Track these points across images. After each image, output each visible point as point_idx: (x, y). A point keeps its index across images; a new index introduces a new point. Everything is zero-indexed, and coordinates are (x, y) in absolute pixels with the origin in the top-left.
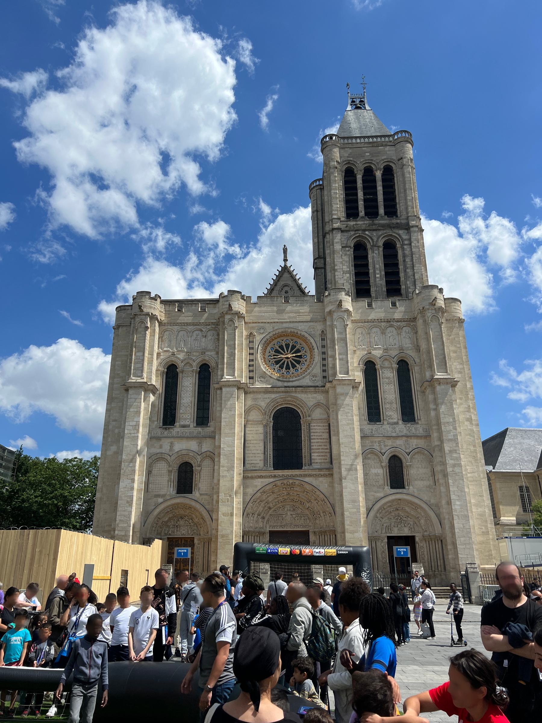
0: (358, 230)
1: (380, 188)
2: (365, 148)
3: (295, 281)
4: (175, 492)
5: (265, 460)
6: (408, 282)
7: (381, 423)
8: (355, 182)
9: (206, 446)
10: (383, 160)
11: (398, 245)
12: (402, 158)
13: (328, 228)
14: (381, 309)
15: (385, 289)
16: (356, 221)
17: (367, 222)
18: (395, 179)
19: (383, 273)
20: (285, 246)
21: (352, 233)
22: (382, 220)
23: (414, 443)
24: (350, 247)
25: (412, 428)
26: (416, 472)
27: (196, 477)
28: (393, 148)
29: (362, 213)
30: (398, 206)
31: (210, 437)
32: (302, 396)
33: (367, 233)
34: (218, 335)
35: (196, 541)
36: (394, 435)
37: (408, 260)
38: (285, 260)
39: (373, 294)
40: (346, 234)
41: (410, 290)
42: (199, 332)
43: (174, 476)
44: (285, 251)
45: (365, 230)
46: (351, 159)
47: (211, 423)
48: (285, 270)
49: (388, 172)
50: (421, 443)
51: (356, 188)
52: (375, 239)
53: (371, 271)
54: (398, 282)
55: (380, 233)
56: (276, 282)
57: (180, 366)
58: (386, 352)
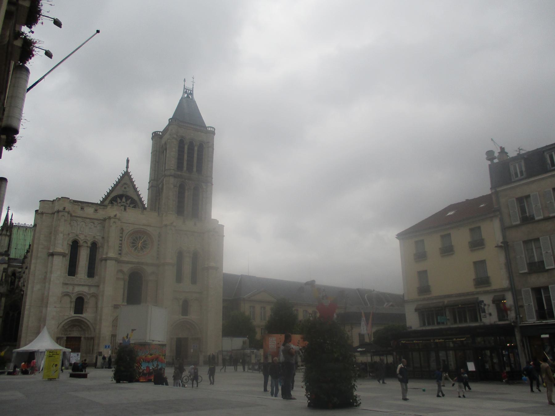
1: (196, 156)
3: (132, 182)
5: (123, 299)
8: (184, 148)
9: (93, 290)
27: (85, 306)
29: (185, 169)
31: (96, 286)
34: (104, 227)
35: (82, 339)
38: (127, 167)
42: (92, 224)
43: (73, 305)
44: (128, 161)
47: (96, 278)
51: (184, 152)
57: (81, 242)
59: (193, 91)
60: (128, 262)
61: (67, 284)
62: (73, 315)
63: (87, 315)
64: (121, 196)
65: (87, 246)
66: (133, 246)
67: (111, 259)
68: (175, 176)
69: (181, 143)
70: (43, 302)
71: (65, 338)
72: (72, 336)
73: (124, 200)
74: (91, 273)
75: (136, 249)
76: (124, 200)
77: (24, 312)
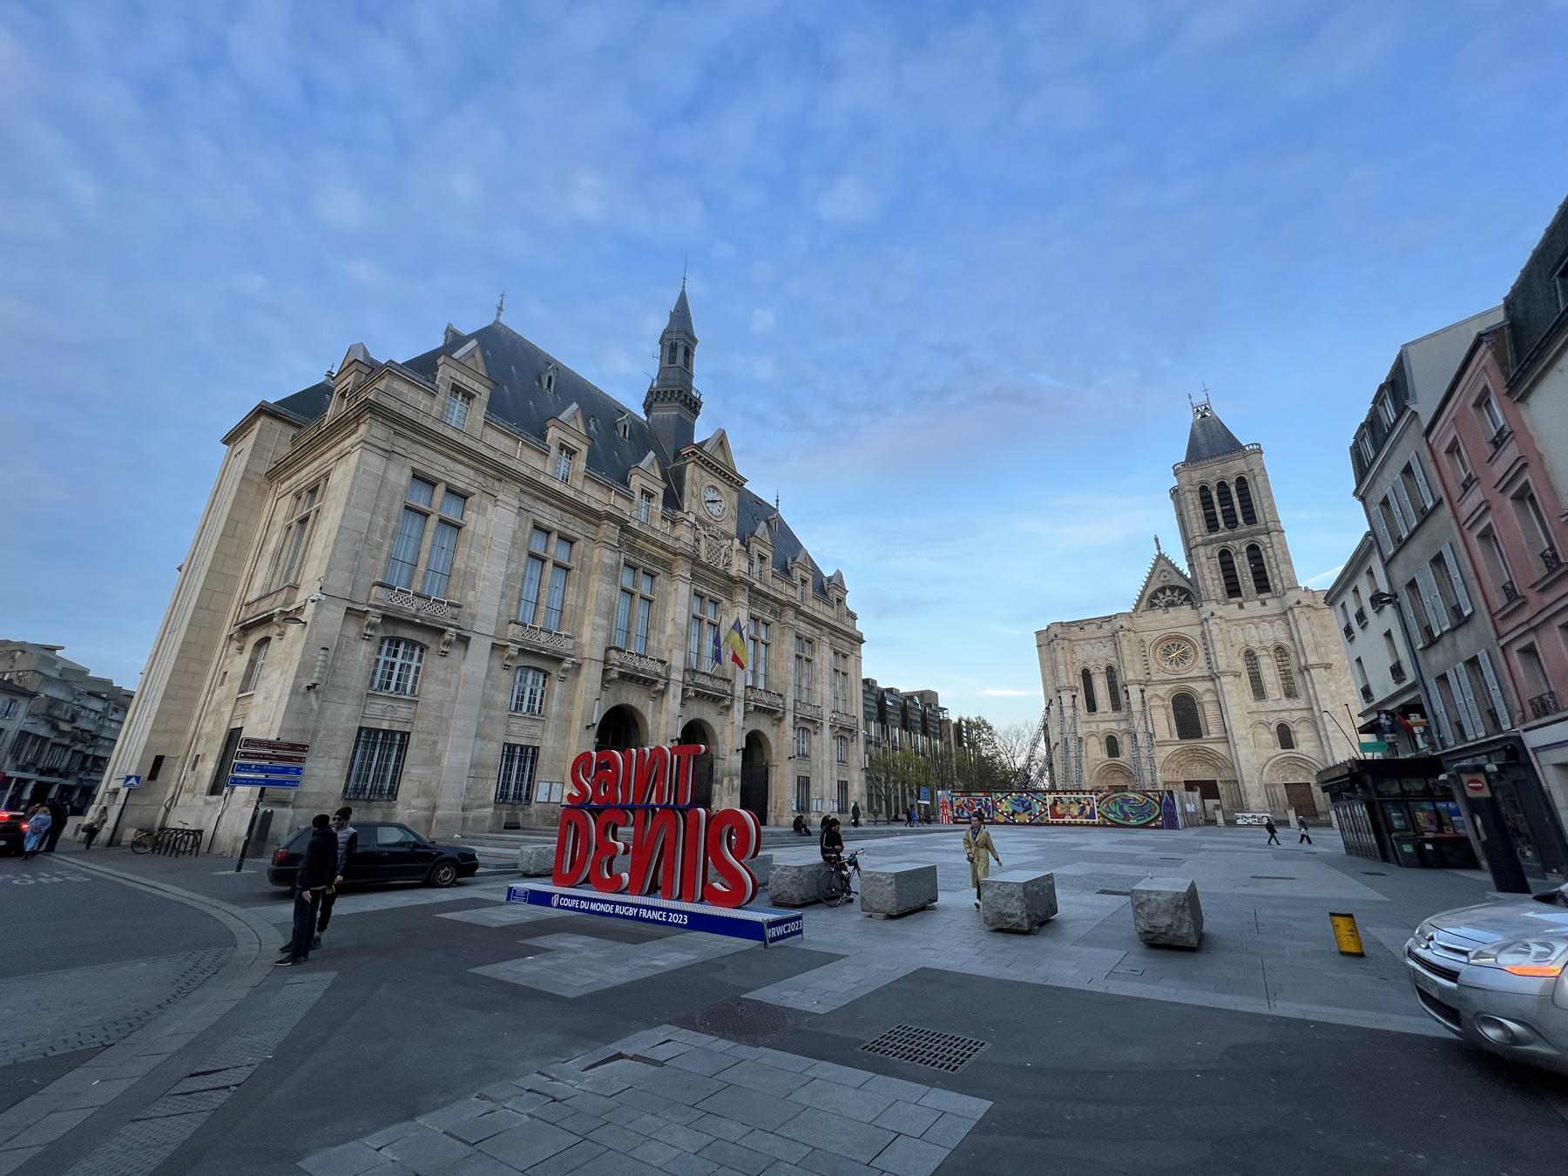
1: (1236, 500)
3: (1173, 566)
9: (1123, 726)
13: (1192, 544)
14: (1253, 607)
17: (1228, 533)
22: (1243, 528)
23: (1297, 715)
25: (1295, 703)
26: (1302, 735)
29: (1222, 525)
32: (1192, 685)
40: (1209, 548)
43: (1104, 746)
44: (1157, 540)
48: (1161, 557)
49: (1241, 482)
50: (1305, 714)
54: (1266, 579)
56: (1153, 570)
57: (1092, 670)
60: (1164, 682)
62: (1105, 756)
63: (1124, 757)
64: (1162, 590)
68: (1205, 544)
69: (1204, 491)
73: (1168, 592)
74: (1116, 706)
76: (1168, 592)
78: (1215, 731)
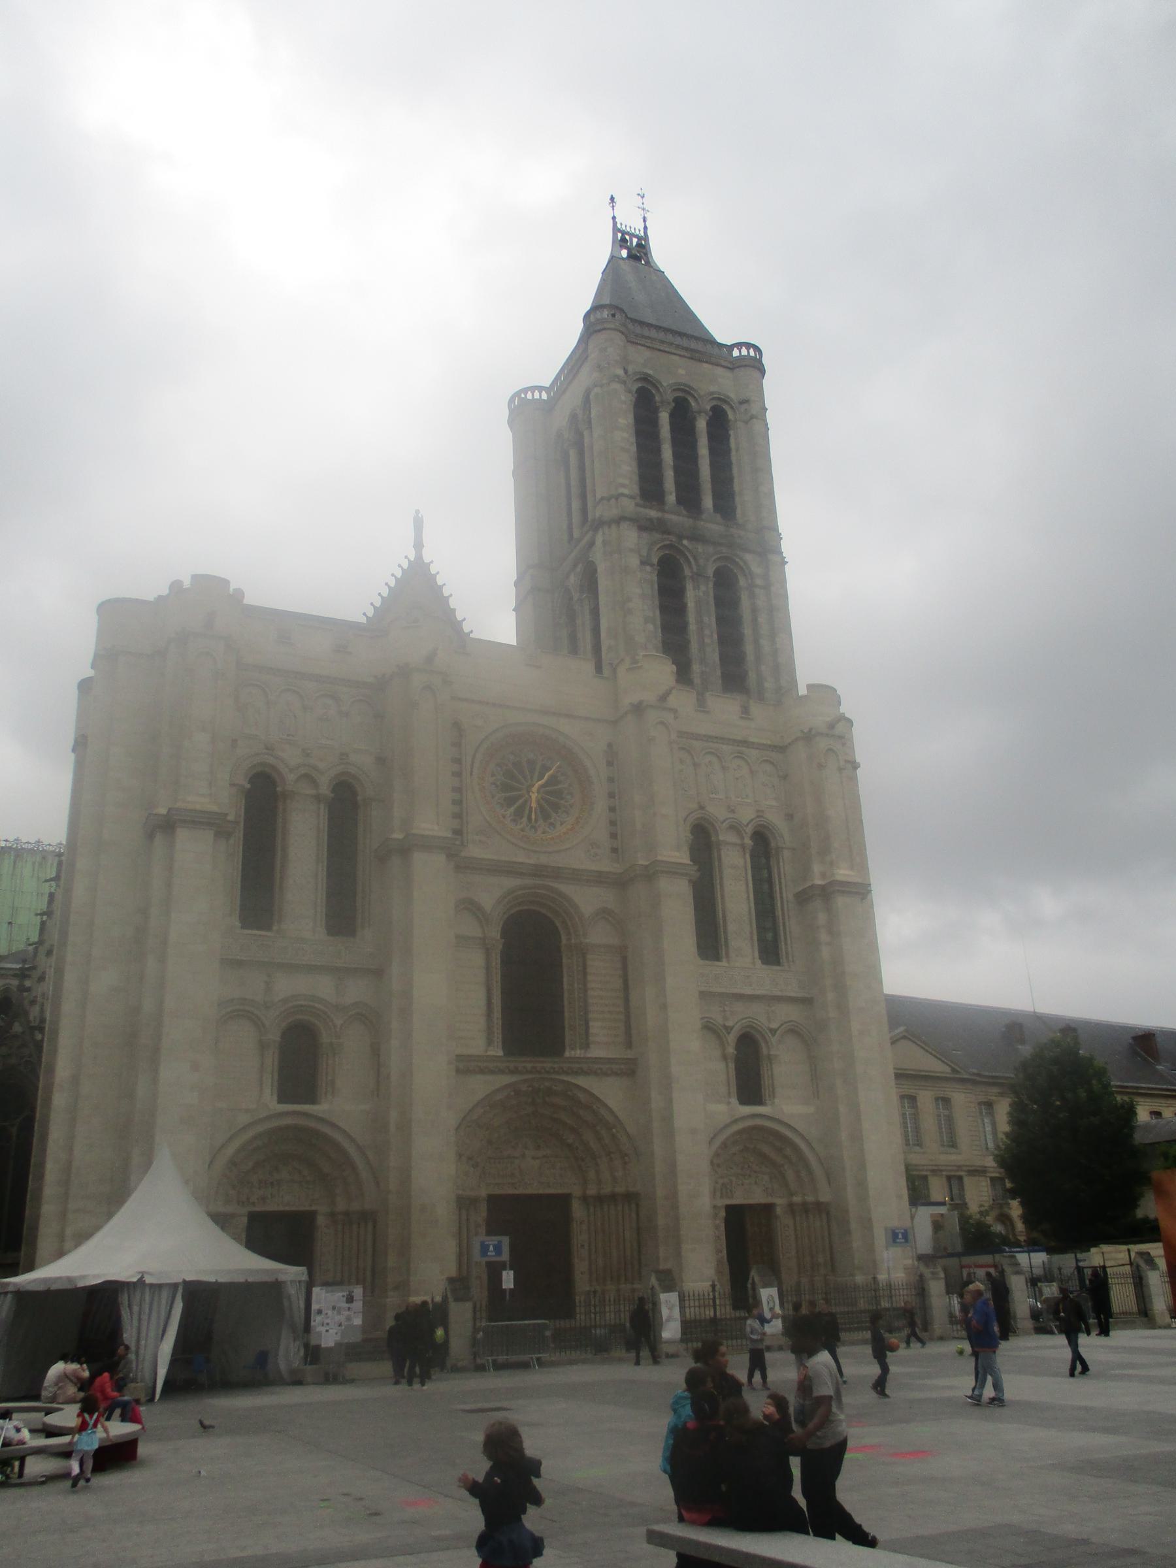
0: (669, 534)
2: (677, 358)
4: (275, 1097)
5: (489, 1029)
6: (763, 668)
7: (724, 963)
9: (356, 991)
10: (712, 393)
11: (742, 582)
12: (746, 401)
15: (719, 673)
16: (663, 511)
18: (732, 440)
19: (715, 636)
20: (417, 512)
21: (657, 536)
24: (652, 565)
28: (728, 374)
29: (671, 498)
30: (737, 499)
33: (685, 542)
35: (321, 1220)
36: (748, 991)
37: (762, 619)
38: (419, 545)
39: (697, 680)
40: (645, 535)
41: (767, 685)
43: (272, 1059)
44: (418, 524)
45: (680, 537)
46: (651, 372)
52: (701, 562)
53: (692, 627)
55: (711, 549)
58: (733, 811)
59: (646, 238)
61: (239, 964)
65: (318, 798)
66: (510, 802)
67: (427, 844)
70: (137, 1044)
71: (245, 1220)
72: (271, 1207)
75: (519, 813)
77: (48, 1100)
78: (602, 1043)
